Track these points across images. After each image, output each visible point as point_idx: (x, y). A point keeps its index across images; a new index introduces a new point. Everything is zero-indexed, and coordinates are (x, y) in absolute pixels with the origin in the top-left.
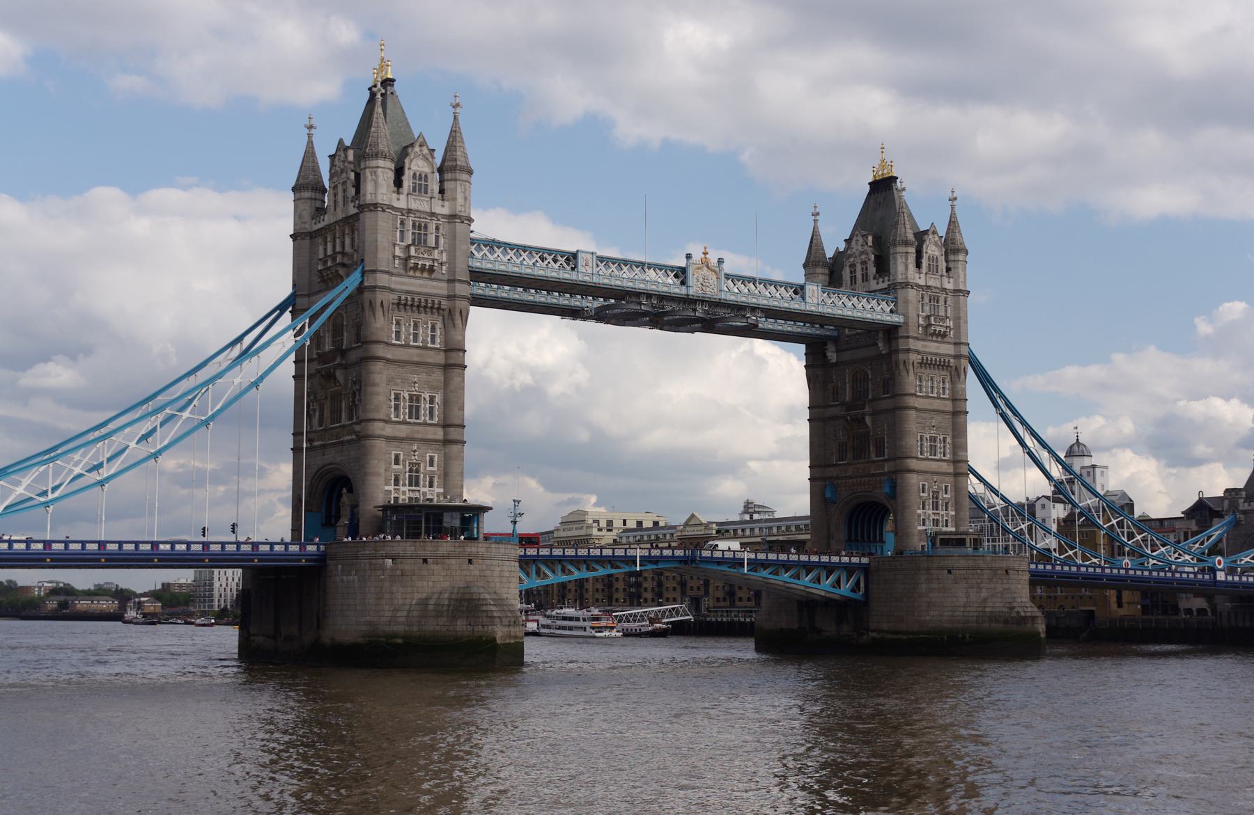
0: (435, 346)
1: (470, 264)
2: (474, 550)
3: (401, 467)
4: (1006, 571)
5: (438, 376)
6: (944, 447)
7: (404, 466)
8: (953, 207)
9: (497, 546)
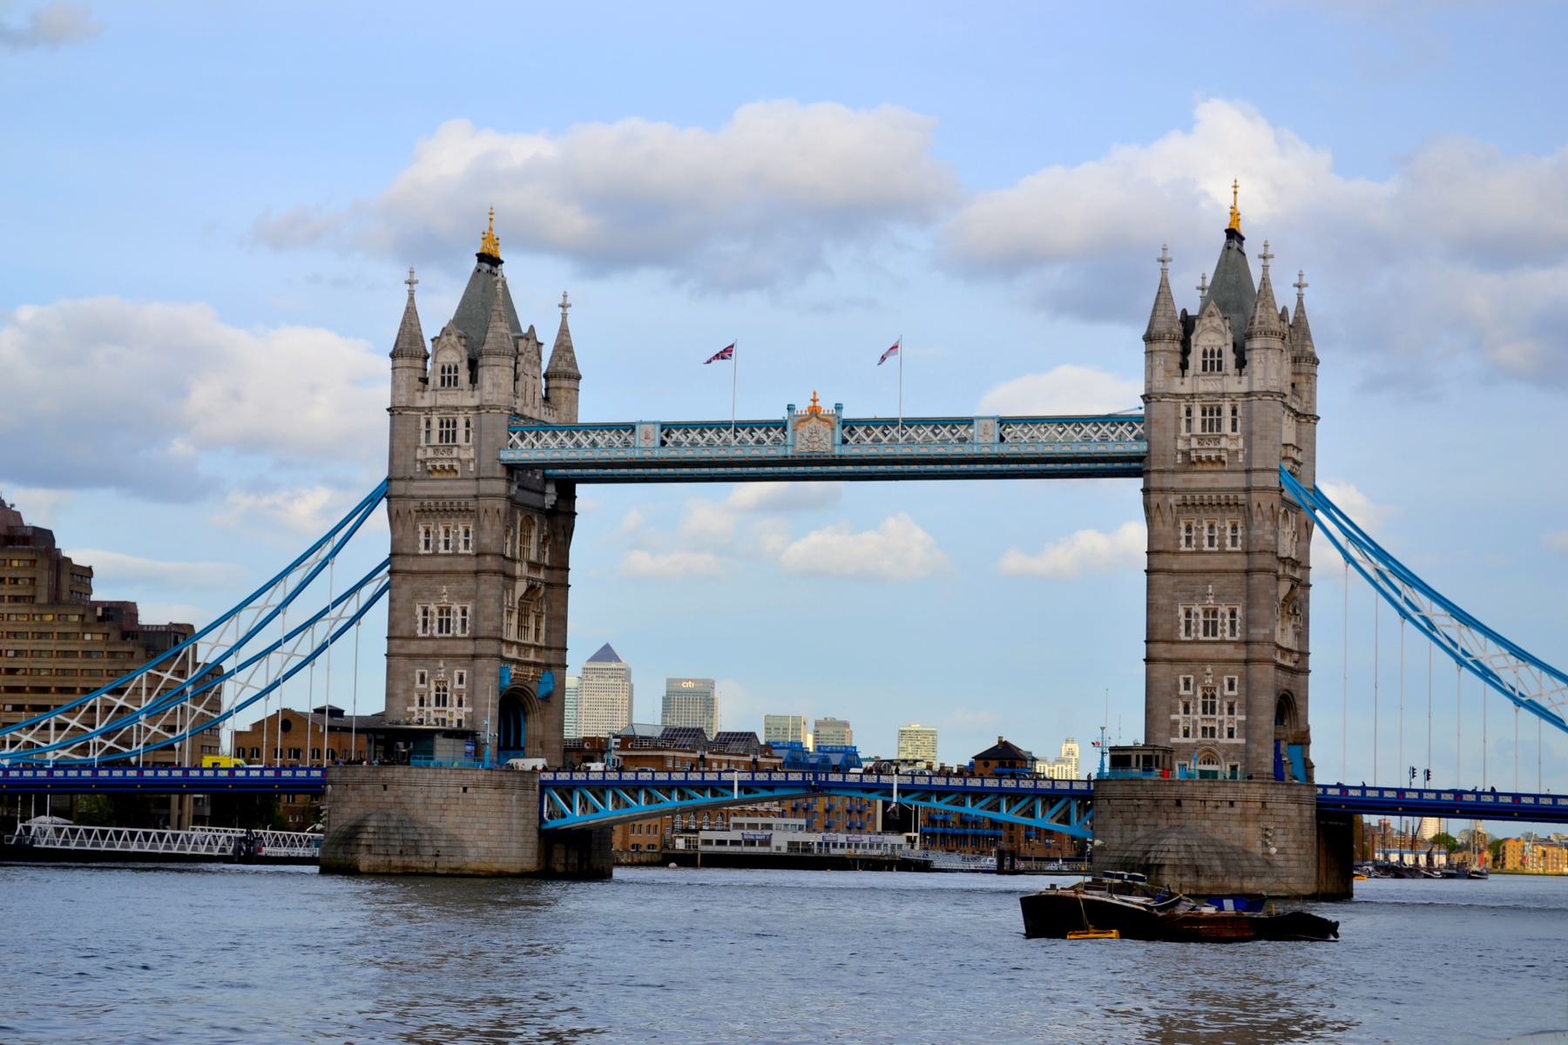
0: (467, 552)
1: (502, 456)
2: (389, 775)
3: (425, 686)
4: (1179, 803)
5: (469, 583)
6: (1233, 624)
7: (429, 685)
8: (1265, 268)
9: (420, 771)
